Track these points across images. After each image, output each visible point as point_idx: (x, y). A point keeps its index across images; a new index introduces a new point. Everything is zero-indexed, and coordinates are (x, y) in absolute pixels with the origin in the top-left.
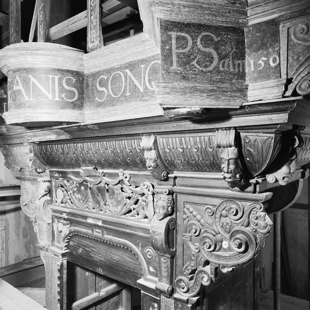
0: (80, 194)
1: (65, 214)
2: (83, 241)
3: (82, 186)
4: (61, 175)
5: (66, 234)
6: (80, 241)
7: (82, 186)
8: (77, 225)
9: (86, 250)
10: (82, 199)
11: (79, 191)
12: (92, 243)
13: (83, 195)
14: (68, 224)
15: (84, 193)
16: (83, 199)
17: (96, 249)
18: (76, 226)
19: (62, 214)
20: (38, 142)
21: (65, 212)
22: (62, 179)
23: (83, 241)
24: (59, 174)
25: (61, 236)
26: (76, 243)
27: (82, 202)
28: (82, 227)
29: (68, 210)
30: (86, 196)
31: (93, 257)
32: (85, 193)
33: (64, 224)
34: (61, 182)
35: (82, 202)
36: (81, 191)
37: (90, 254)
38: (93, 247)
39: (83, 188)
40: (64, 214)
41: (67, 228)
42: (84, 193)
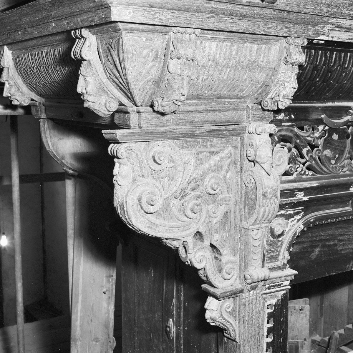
0: (329, 148)
1: (302, 193)
2: (322, 234)
3: (334, 134)
4: (293, 117)
5: (296, 233)
6: (316, 236)
7: (334, 134)
8: (321, 207)
9: (329, 246)
10: (335, 157)
11: (328, 144)
12: (340, 228)
13: (335, 149)
14: (297, 214)
15: (338, 146)
16: (337, 156)
17: (348, 234)
18: (319, 210)
19: (294, 196)
20: (323, 42)
21: (300, 190)
22: (290, 124)
23: (322, 234)
24: (287, 113)
25: (279, 244)
26: (306, 245)
27: (333, 162)
28: (331, 206)
29: (317, 183)
30: (342, 149)
31: (342, 250)
32: (341, 145)
33: (288, 217)
34: (287, 130)
35: (333, 162)
36: (332, 142)
37: (337, 248)
38: (341, 235)
39: (335, 137)
40: (299, 193)
41: (296, 220)
42: (338, 146)
